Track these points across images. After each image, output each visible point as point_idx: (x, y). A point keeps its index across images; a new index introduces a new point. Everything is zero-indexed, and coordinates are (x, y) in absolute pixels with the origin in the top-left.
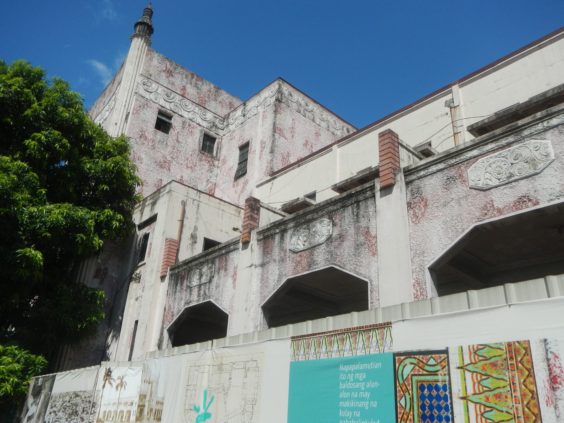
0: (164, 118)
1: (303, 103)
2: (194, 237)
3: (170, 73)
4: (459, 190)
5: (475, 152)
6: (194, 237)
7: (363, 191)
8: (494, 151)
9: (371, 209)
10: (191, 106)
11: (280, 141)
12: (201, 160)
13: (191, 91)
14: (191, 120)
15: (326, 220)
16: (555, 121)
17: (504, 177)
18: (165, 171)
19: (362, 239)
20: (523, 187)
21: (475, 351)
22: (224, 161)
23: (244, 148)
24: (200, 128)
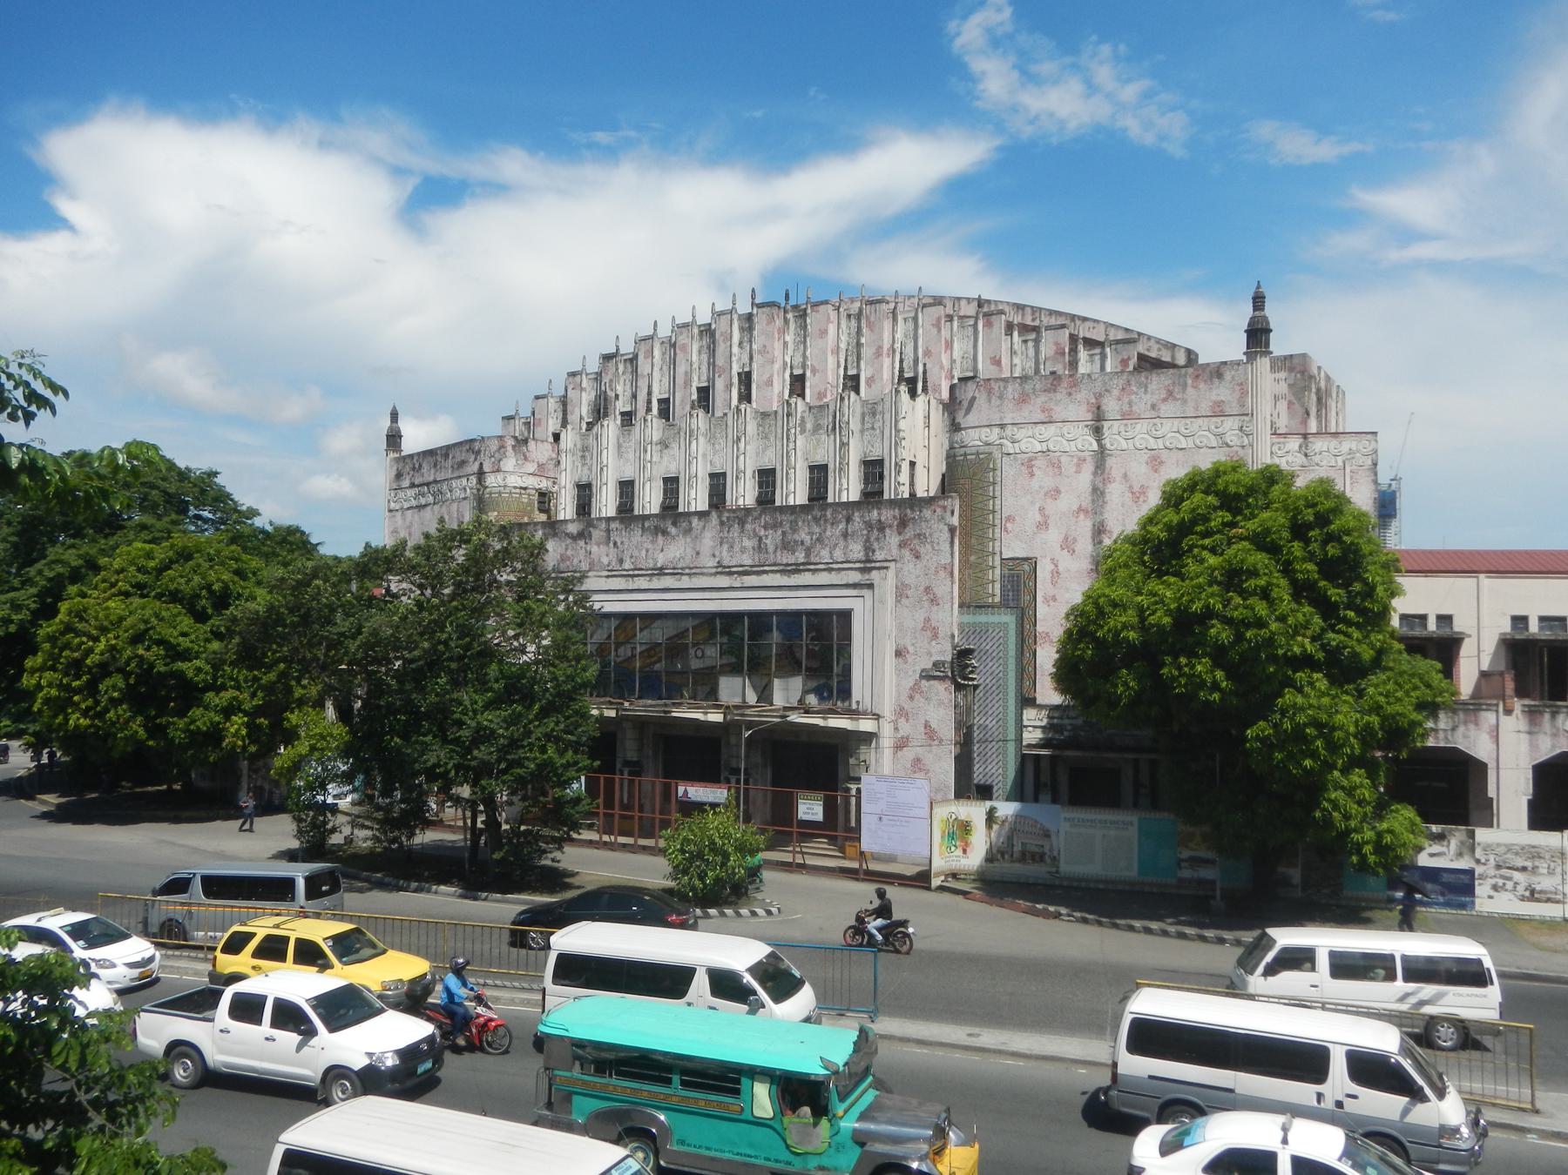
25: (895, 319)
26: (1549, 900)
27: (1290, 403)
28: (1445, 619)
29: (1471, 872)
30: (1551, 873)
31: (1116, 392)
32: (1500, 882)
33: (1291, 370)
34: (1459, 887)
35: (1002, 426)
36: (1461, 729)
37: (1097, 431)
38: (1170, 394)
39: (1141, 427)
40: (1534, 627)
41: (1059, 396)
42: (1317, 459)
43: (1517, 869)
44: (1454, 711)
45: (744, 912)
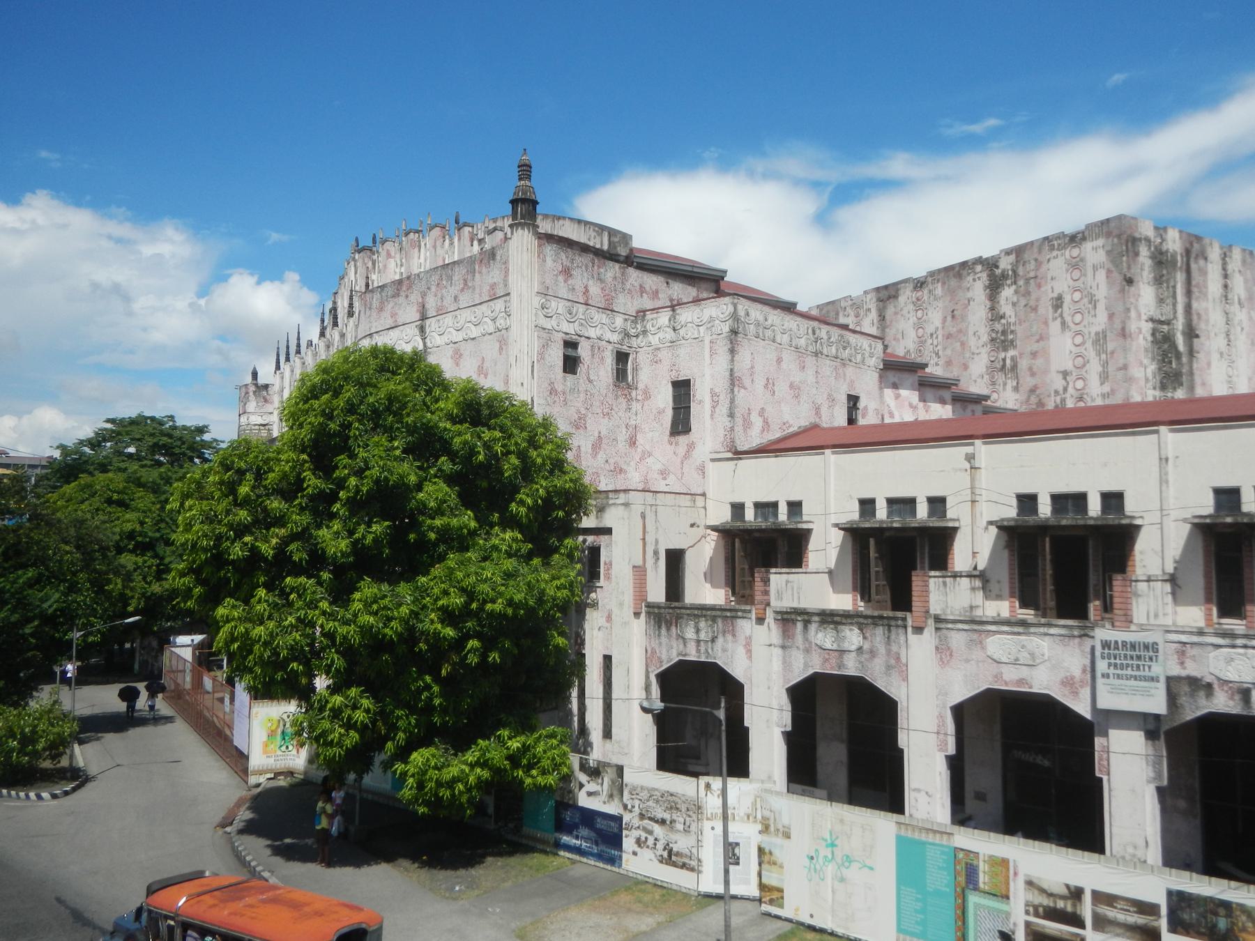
0: (570, 352)
1: (761, 318)
2: (656, 553)
3: (567, 272)
4: (977, 654)
5: (993, 628)
6: (656, 553)
7: (896, 619)
8: (1008, 633)
9: (902, 638)
10: (600, 317)
11: (740, 394)
12: (617, 397)
13: (595, 289)
14: (599, 339)
15: (856, 631)
16: (1053, 631)
17: (1012, 658)
18: (581, 431)
19: (893, 662)
20: (1024, 672)
21: (991, 857)
22: (647, 395)
23: (682, 389)
24: (610, 347)
25: (420, 247)
26: (684, 866)
27: (1109, 272)
28: (795, 507)
29: (619, 819)
30: (687, 831)
31: (433, 289)
32: (644, 835)
33: (1108, 234)
34: (607, 835)
35: (371, 335)
36: (720, 640)
37: (422, 329)
38: (465, 281)
39: (448, 320)
40: (882, 513)
41: (401, 299)
42: (682, 332)
43: (657, 822)
44: (714, 619)
45: (32, 795)
